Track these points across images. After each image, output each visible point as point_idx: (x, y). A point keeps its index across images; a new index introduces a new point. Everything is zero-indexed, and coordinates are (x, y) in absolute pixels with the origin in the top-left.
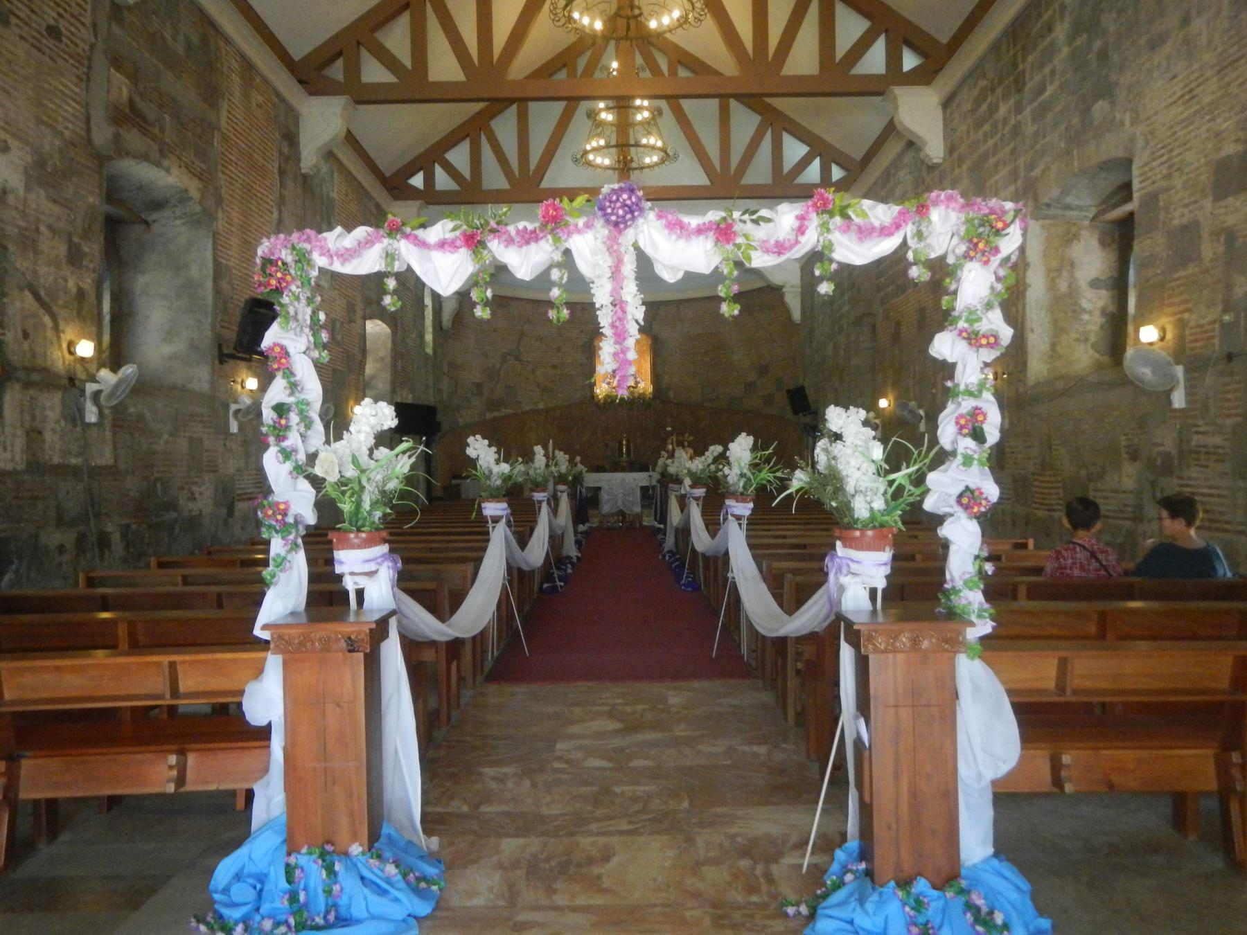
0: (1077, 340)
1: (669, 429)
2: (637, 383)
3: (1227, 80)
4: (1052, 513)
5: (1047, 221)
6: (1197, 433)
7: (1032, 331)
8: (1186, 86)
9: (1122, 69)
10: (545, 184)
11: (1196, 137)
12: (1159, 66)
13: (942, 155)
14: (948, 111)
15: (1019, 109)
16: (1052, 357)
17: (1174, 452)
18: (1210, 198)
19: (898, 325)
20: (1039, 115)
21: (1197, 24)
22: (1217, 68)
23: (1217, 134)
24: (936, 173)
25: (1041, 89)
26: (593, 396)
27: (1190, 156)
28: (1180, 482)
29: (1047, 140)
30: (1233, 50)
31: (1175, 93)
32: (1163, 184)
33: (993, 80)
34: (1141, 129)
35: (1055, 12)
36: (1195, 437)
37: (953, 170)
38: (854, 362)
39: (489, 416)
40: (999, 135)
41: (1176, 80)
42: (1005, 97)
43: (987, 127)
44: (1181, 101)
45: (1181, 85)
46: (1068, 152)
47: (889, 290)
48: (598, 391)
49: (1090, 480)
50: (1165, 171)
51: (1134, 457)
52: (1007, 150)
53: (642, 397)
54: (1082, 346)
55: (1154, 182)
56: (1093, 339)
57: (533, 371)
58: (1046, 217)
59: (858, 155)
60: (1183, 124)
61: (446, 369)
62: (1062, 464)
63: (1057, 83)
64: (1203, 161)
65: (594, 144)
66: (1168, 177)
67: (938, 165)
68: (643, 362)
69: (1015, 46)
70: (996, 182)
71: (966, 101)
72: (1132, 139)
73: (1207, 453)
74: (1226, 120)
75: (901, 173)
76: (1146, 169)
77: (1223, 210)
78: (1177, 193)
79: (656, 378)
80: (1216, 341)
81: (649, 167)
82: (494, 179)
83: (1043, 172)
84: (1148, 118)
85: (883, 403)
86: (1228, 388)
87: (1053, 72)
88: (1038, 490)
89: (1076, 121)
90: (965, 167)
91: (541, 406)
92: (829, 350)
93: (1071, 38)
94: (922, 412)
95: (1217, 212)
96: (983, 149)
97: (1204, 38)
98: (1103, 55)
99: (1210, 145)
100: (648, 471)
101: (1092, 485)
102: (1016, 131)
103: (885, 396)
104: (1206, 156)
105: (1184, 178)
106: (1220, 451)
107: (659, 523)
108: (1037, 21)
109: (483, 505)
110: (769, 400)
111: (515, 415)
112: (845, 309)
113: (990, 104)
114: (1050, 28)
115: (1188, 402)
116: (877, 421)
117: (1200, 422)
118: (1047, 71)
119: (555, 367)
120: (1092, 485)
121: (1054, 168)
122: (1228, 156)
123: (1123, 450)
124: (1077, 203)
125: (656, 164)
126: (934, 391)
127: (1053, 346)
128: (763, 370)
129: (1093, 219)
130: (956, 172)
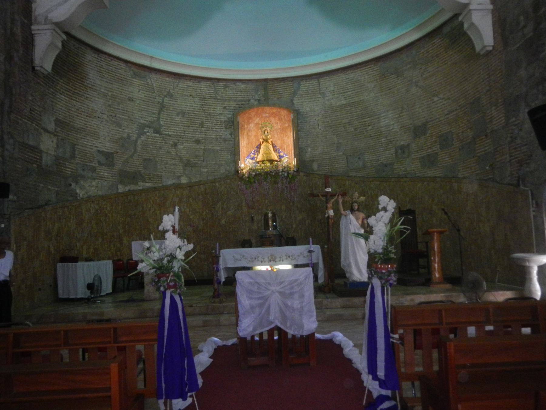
2: (280, 157)
26: (237, 171)
39: (121, 189)
48: (242, 166)
53: (286, 169)
57: (175, 145)
61: (51, 126)
68: (285, 138)
79: (299, 151)
91: (184, 180)
100: (309, 244)
107: (383, 384)
111: (155, 189)
119: (198, 142)
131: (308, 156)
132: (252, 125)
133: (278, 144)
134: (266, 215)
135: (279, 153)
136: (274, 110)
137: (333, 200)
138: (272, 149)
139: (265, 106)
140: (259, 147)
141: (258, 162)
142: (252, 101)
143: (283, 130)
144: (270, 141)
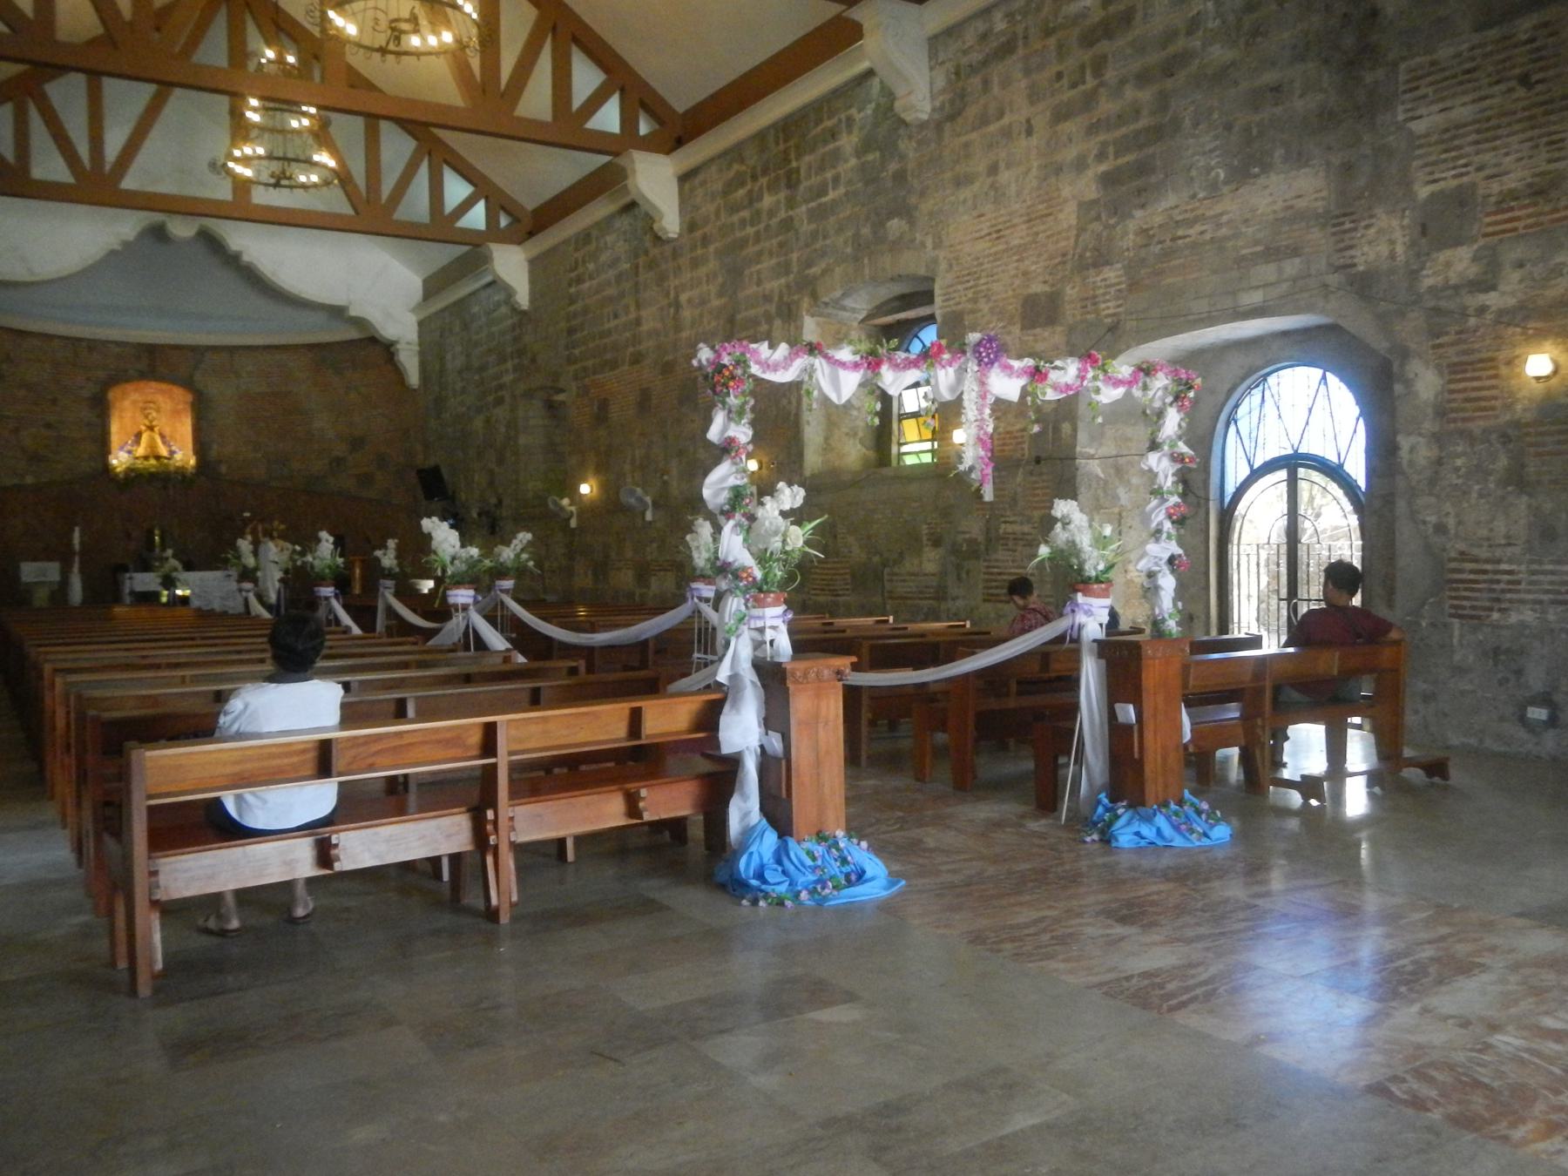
0: (847, 434)
1: (247, 514)
2: (172, 453)
3: (1035, 229)
4: (839, 598)
5: (821, 319)
6: (1005, 522)
7: (808, 423)
8: (992, 226)
9: (922, 194)
10: (129, 183)
11: (1003, 271)
12: (965, 201)
13: (678, 230)
14: (687, 186)
15: (791, 203)
16: (825, 449)
17: (981, 539)
18: (1018, 326)
19: (604, 405)
20: (818, 214)
21: (1005, 176)
22: (1025, 218)
23: (1025, 274)
24: (668, 249)
25: (822, 191)
26: (106, 469)
27: (996, 287)
28: (986, 564)
29: (828, 242)
30: (1040, 207)
31: (981, 230)
32: (969, 306)
33: (754, 168)
34: (942, 254)
35: (840, 120)
36: (1003, 526)
37: (693, 248)
38: (522, 440)
40: (762, 226)
41: (982, 219)
42: (772, 188)
43: (745, 214)
44: (988, 238)
45: (988, 224)
46: (856, 259)
47: (590, 363)
48: (115, 462)
49: (885, 566)
50: (970, 295)
51: (936, 542)
52: (774, 242)
53: (181, 471)
54: (851, 442)
55: (959, 303)
56: (861, 434)
57: (16, 431)
58: (821, 315)
59: (530, 203)
60: (991, 258)
62: (850, 552)
63: (842, 190)
64: (1010, 293)
65: (248, 150)
66: (975, 300)
67: (673, 240)
69: (786, 141)
70: (759, 272)
71: (715, 179)
72: (935, 261)
73: (1015, 539)
74: (1036, 263)
75: (609, 239)
76: (951, 290)
77: (1031, 338)
78: (983, 316)
79: (200, 447)
80: (1026, 446)
81: (304, 186)
82: (49, 166)
83: (824, 272)
84: (951, 246)
85: (585, 489)
86: (1037, 485)
87: (836, 179)
88: (815, 576)
89: (866, 231)
90: (712, 248)
91: (29, 480)
92: (478, 423)
93: (860, 152)
94: (648, 500)
95: (1026, 338)
96: (739, 234)
97: (1013, 188)
98: (900, 177)
99: (1017, 282)
101: (887, 571)
102: (787, 225)
103: (585, 481)
104: (1014, 290)
105: (991, 304)
106: (1029, 537)
108: (817, 125)
109: (450, 593)
110: (366, 480)
112: (508, 378)
113: (751, 191)
114: (833, 134)
115: (995, 496)
116: (573, 508)
117: (1008, 513)
118: (829, 175)
119: (48, 426)
120: (887, 571)
121: (838, 270)
122: (1036, 294)
123: (925, 538)
124: (853, 305)
125: (315, 185)
126: (666, 477)
127: (826, 439)
128: (357, 443)
129: (862, 321)
130: (699, 252)
131: (214, 452)
132: (127, 403)
133: (167, 431)
134: (150, 533)
135: (170, 446)
136: (164, 386)
137: (250, 526)
138: (159, 440)
139: (150, 380)
140: (138, 436)
141: (137, 458)
142: (131, 372)
143: (176, 413)
144: (156, 429)
